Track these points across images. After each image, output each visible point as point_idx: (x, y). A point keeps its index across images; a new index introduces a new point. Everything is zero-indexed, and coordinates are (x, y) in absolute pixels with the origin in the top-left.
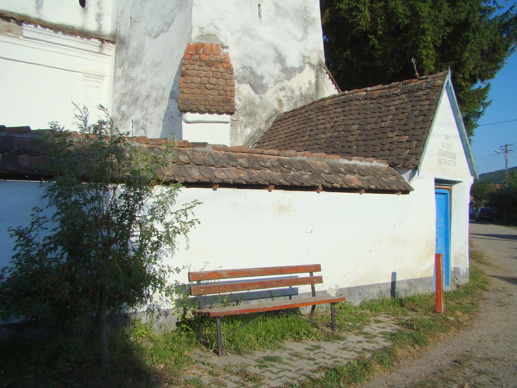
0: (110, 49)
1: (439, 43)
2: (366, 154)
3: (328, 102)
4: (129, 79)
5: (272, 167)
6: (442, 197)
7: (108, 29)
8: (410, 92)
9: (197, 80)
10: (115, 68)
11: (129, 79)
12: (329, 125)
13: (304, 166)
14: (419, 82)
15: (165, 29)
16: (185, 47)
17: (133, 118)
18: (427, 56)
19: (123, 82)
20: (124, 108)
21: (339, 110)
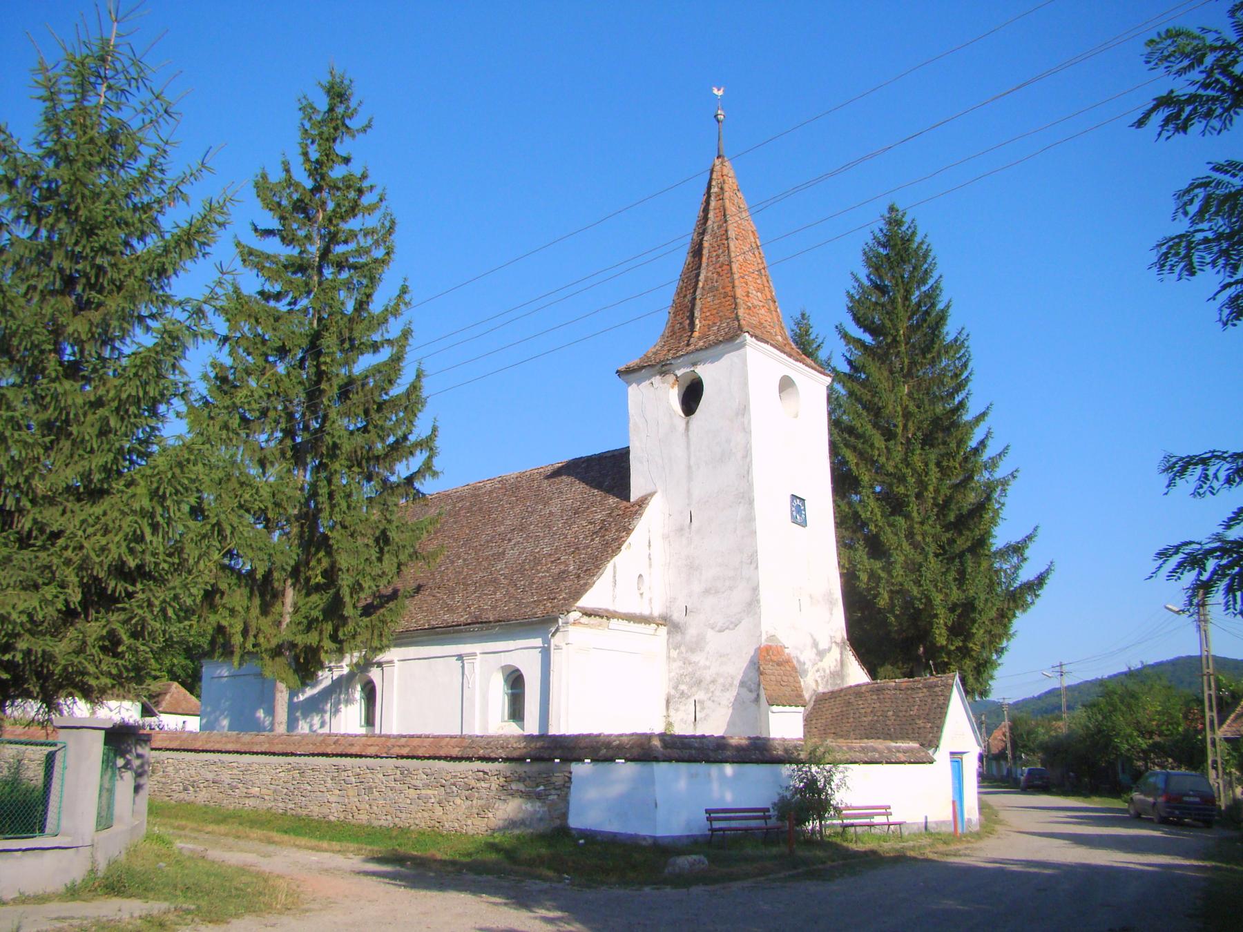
0: (663, 630)
1: (950, 624)
2: (904, 736)
3: (864, 688)
4: (687, 662)
5: (860, 752)
6: (956, 764)
7: (656, 613)
8: (930, 687)
9: (773, 678)
10: (669, 650)
11: (687, 662)
12: (869, 710)
13: (875, 750)
14: (936, 680)
15: (731, 627)
16: (755, 646)
17: (697, 697)
18: (940, 635)
19: (680, 663)
20: (683, 687)
21: (875, 697)
